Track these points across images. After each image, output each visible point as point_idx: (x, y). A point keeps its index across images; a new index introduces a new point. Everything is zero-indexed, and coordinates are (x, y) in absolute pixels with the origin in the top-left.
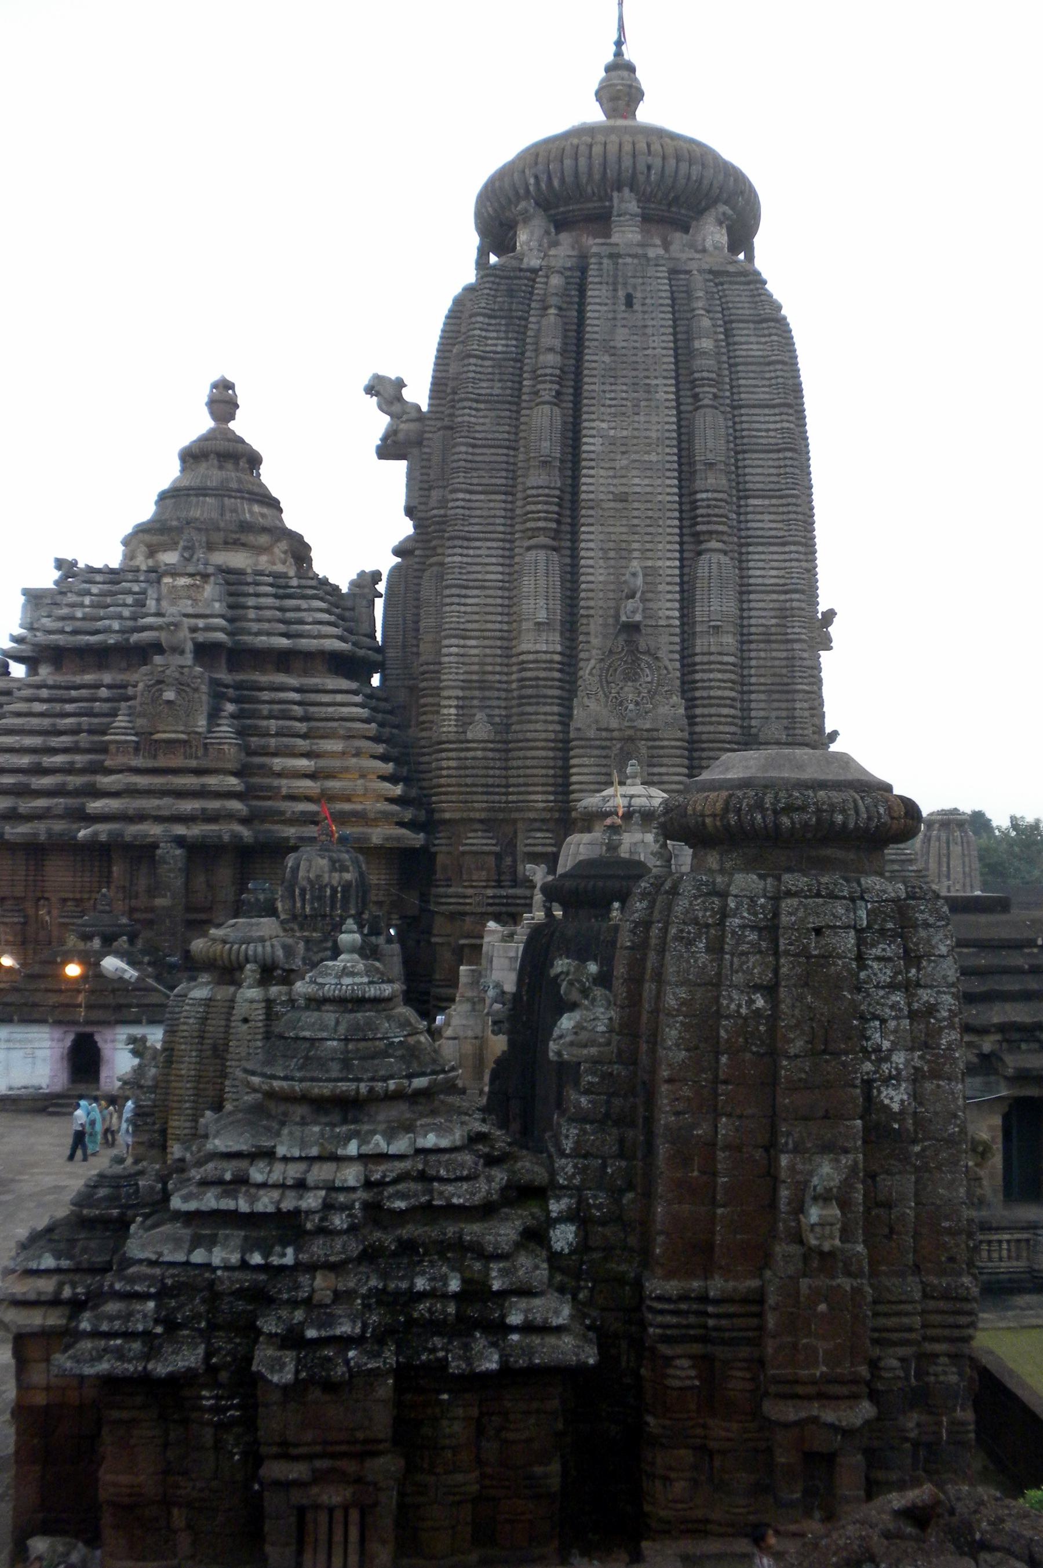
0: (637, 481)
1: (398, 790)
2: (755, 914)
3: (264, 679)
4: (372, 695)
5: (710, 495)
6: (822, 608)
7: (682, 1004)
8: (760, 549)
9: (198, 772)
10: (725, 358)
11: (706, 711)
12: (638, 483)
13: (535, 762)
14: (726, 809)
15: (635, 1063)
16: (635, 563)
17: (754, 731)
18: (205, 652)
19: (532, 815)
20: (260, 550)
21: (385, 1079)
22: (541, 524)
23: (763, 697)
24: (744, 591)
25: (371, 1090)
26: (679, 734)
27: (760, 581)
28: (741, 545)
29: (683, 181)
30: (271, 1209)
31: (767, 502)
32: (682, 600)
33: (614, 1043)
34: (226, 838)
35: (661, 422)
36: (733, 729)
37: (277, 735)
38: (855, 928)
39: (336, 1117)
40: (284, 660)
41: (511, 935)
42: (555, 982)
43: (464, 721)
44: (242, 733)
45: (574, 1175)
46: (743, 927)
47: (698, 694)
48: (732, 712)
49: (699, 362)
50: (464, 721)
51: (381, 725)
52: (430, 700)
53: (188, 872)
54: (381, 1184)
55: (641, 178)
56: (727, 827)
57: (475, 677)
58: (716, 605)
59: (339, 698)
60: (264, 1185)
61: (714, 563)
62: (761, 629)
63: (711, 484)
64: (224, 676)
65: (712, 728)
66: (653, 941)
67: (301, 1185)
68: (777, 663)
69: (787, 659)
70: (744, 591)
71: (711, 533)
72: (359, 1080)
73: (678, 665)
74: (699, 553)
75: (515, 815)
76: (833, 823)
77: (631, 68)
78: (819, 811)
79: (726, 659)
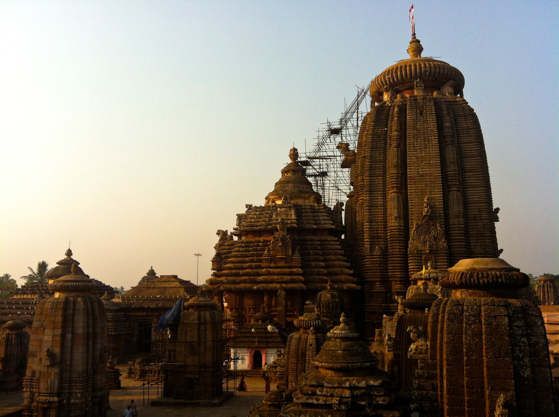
0: (427, 170)
1: (351, 272)
2: (473, 311)
3: (308, 238)
4: (342, 241)
5: (452, 173)
6: (494, 207)
7: (451, 340)
8: (471, 189)
9: (289, 267)
10: (455, 128)
11: (455, 244)
12: (427, 170)
13: (396, 262)
14: (461, 278)
15: (436, 360)
16: (427, 196)
17: (472, 250)
18: (290, 230)
19: (395, 279)
20: (306, 198)
21: (356, 363)
22: (395, 185)
23: (475, 238)
24: (465, 203)
25: (352, 366)
26: (445, 252)
27: (471, 200)
28: (464, 188)
29: (437, 75)
30: (323, 403)
31: (472, 174)
32: (444, 208)
33: (429, 353)
34: (298, 288)
35: (434, 150)
36: (464, 250)
37: (313, 255)
38: (507, 316)
39: (341, 374)
40: (314, 232)
41: (392, 319)
42: (408, 334)
43: (372, 249)
44: (302, 255)
45: (417, 397)
46: (469, 315)
47: (451, 238)
48: (464, 244)
49: (446, 130)
50: (372, 249)
51: (345, 251)
52: (361, 242)
53: (286, 300)
54: (357, 396)
55: (423, 75)
56: (462, 283)
57: (375, 235)
58: (456, 209)
59: (332, 243)
60: (321, 395)
61: (454, 195)
62: (473, 216)
63: (452, 169)
64: (296, 237)
65: (457, 249)
66: (440, 320)
67: (332, 396)
68: (479, 227)
69: (483, 225)
70: (465, 203)
71: (453, 185)
72: (349, 363)
73: (444, 229)
74: (450, 192)
75: (391, 279)
76: (497, 281)
77: (418, 41)
78: (493, 278)
79: (461, 226)
